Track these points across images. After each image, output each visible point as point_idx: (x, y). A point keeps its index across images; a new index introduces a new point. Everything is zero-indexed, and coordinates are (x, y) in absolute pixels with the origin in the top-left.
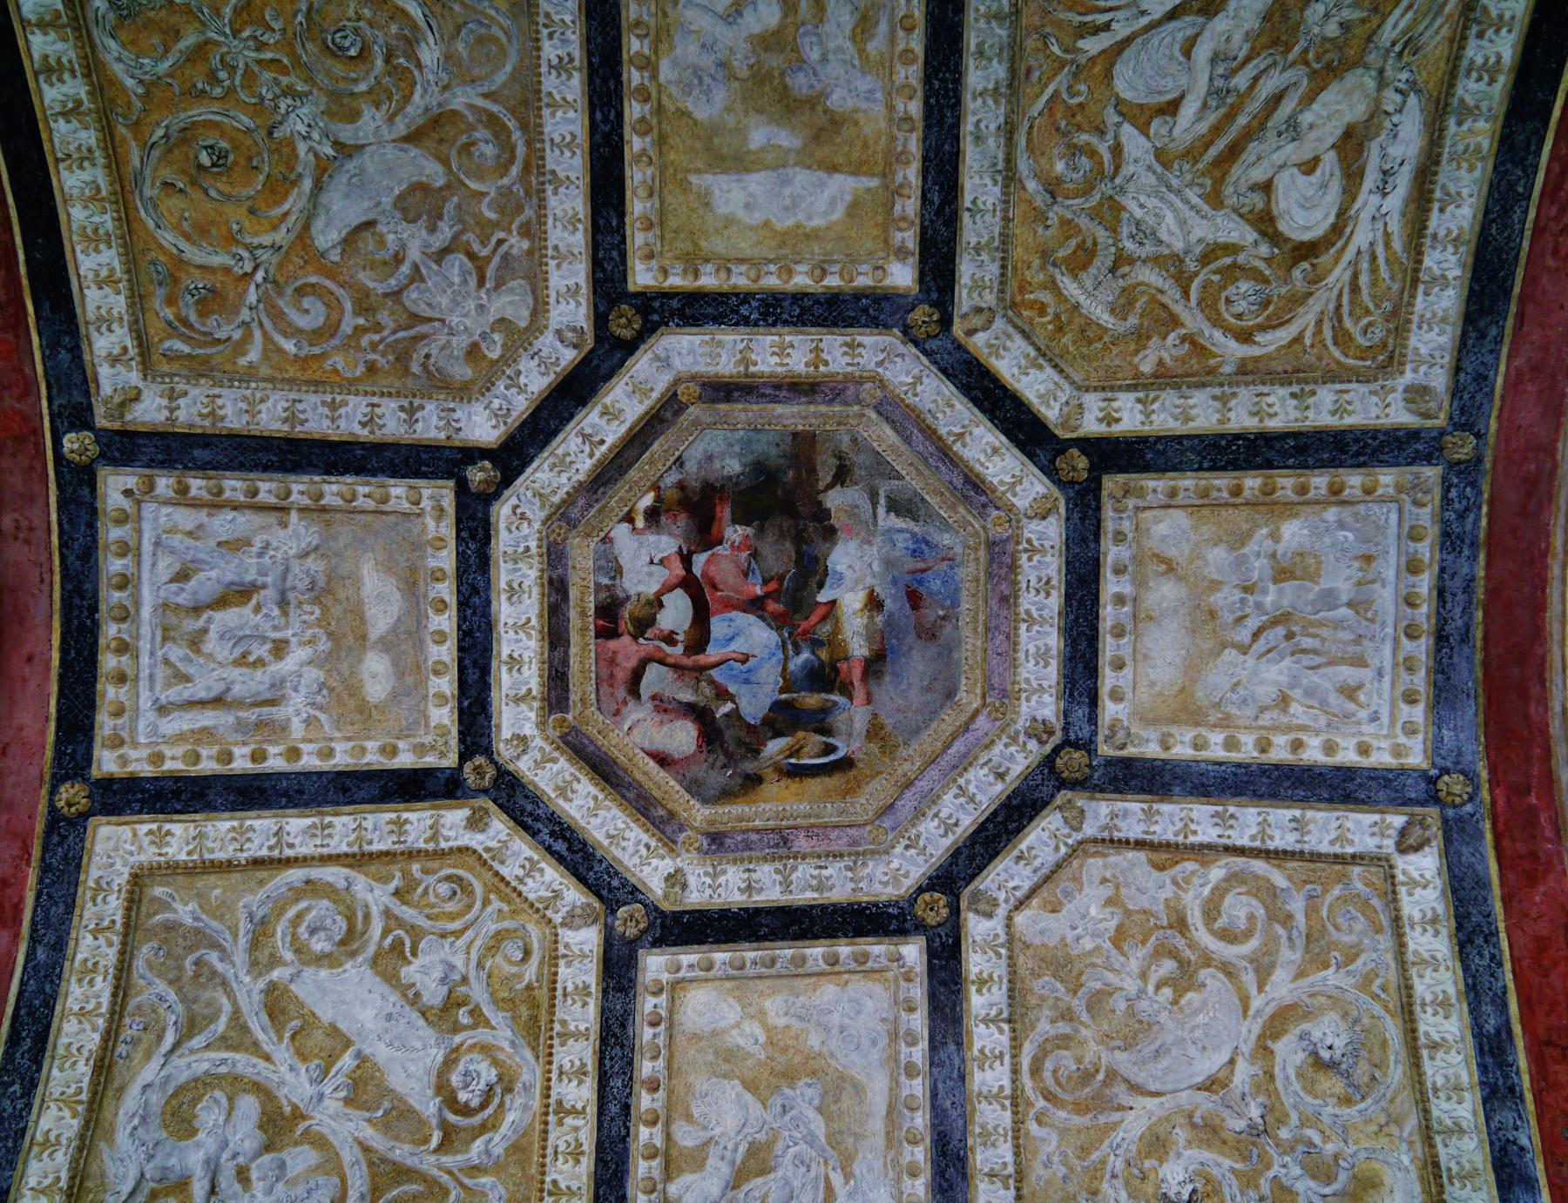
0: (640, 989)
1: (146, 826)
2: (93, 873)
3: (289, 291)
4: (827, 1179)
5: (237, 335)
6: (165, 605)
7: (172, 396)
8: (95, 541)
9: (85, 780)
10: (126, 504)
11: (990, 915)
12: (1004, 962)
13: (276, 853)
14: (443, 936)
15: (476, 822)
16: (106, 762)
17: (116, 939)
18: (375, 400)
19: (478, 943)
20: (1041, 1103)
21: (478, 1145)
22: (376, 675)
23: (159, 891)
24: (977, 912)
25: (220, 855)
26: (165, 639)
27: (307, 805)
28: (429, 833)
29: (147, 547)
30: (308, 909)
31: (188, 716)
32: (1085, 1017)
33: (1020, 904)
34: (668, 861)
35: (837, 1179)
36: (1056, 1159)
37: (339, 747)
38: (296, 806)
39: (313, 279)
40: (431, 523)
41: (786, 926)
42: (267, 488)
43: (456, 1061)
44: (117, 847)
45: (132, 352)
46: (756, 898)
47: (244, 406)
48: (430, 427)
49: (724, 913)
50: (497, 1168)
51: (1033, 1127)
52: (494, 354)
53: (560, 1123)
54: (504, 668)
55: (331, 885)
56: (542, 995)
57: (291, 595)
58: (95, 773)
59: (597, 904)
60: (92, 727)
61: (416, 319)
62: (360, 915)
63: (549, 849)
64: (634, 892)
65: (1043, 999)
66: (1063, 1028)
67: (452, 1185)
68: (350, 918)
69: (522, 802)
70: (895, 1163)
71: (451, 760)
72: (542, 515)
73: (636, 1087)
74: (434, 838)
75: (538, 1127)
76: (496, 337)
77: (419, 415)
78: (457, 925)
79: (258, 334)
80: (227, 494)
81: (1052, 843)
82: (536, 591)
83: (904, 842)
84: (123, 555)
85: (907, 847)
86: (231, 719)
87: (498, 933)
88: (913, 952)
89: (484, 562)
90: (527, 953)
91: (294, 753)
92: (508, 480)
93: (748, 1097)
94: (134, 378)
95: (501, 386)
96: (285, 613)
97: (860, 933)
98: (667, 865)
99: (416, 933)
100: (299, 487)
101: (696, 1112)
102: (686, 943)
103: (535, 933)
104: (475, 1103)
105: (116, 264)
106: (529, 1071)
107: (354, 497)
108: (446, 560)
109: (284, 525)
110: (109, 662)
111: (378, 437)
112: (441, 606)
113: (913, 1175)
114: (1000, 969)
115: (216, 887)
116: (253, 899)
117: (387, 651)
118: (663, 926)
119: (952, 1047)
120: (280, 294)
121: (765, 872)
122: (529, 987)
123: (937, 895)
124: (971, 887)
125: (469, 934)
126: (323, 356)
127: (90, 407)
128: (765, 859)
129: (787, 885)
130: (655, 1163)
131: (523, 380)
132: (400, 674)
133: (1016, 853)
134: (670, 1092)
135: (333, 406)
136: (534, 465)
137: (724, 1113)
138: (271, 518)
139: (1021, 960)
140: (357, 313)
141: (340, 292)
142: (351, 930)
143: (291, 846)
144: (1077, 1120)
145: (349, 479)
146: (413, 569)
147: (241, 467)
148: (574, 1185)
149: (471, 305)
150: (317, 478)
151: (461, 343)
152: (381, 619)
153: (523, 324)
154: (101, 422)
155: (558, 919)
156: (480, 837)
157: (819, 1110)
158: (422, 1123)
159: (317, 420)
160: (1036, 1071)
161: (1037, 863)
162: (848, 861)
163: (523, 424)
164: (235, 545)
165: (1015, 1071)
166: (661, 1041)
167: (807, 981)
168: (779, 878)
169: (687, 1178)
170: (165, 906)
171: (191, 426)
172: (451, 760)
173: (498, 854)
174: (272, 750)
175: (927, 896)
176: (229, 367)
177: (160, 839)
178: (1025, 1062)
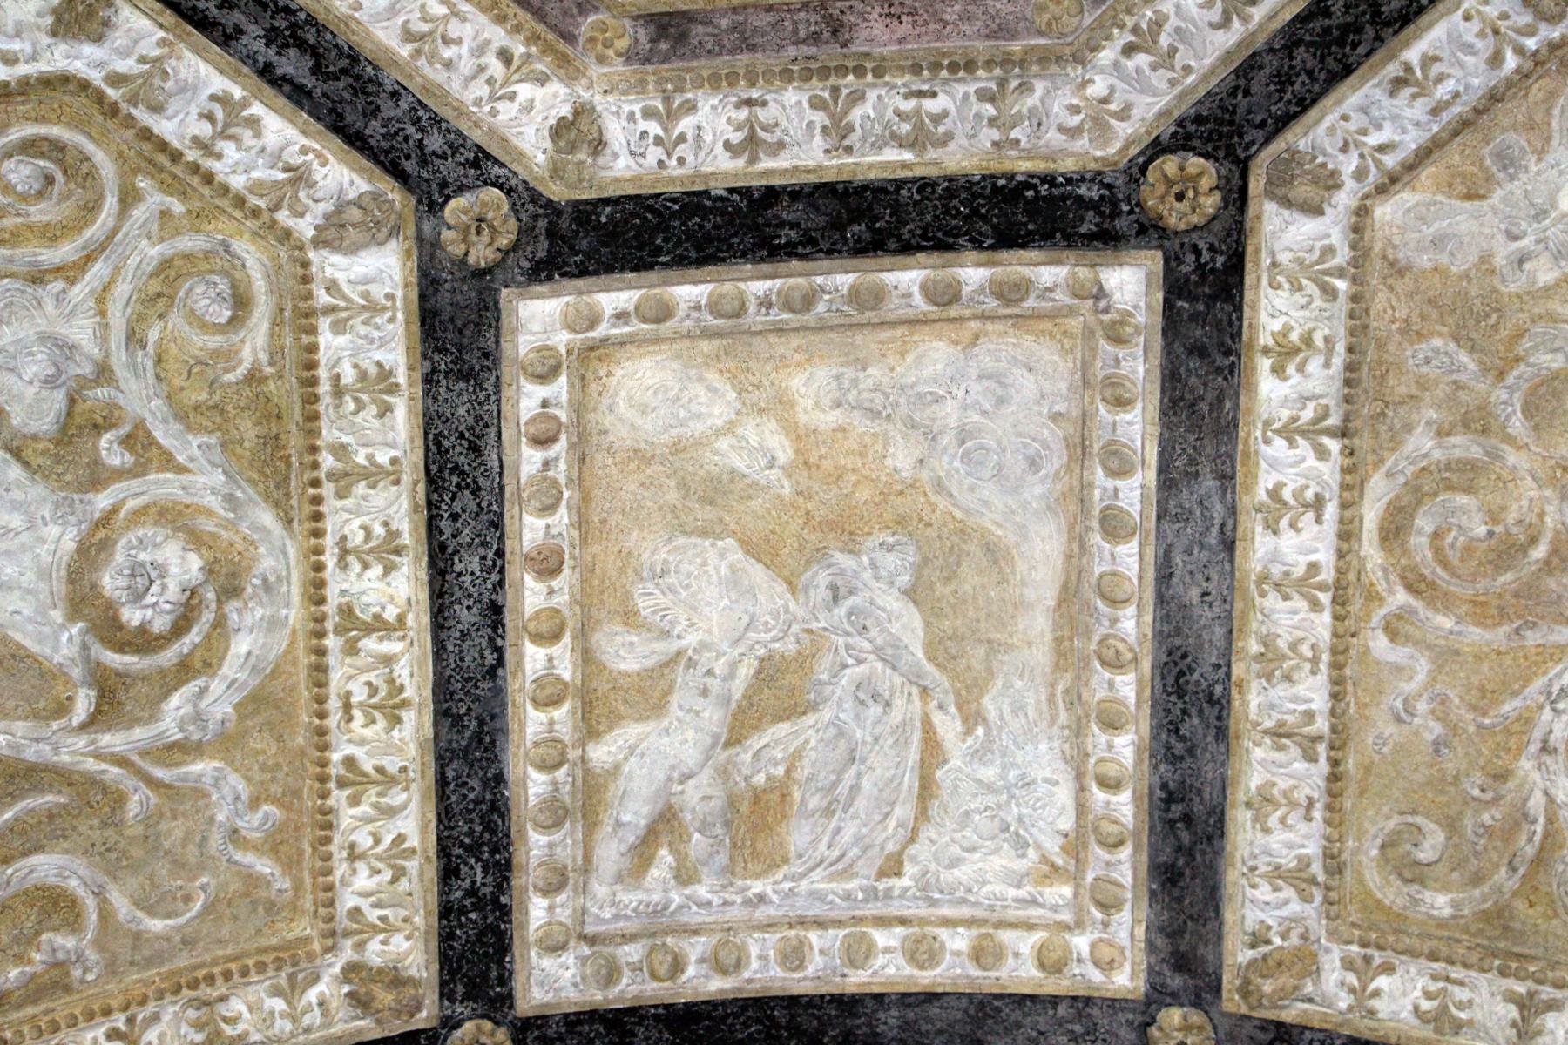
0: (507, 371)
4: (927, 726)
11: (1314, 210)
12: (1342, 305)
14: (37, 278)
19: (122, 289)
20: (1401, 597)
21: (177, 704)
24: (1286, 203)
32: (1517, 425)
33: (1390, 183)
34: (556, 88)
35: (948, 726)
36: (1422, 706)
41: (838, 225)
43: (106, 546)
46: (767, 163)
49: (694, 203)
50: (227, 743)
51: (1380, 645)
53: (351, 649)
56: (284, 391)
59: (394, 193)
63: (266, 72)
64: (481, 163)
65: (1423, 384)
66: (1464, 446)
67: (129, 782)
70: (1074, 699)
73: (511, 573)
75: (305, 660)
78: (66, 251)
81: (1485, 46)
83: (1123, 38)
85: (1129, 50)
87: (165, 264)
88: (1130, 282)
90: (241, 302)
93: (757, 573)
97: (1009, 239)
98: (550, 99)
101: (644, 605)
102: (609, 269)
103: (252, 257)
104: (160, 625)
106: (274, 550)
113: (1111, 724)
114: (1331, 325)
118: (552, 233)
119: (1210, 483)
121: (790, 107)
122: (254, 377)
123: (1195, 163)
124: (1278, 146)
125: (99, 270)
128: (787, 76)
129: (838, 133)
130: (561, 713)
133: (1393, 69)
134: (587, 572)
137: (709, 604)
139: (1380, 301)
144: (1475, 633)
148: (392, 764)
155: (305, 228)
156: (88, 49)
157: (911, 594)
158: (48, 675)
160: (1394, 530)
161: (1442, 91)
162: (985, 79)
165: (1347, 534)
166: (560, 472)
167: (886, 334)
168: (819, 118)
169: (630, 732)
173: (148, 86)
175: (1169, 165)
178: (1371, 515)
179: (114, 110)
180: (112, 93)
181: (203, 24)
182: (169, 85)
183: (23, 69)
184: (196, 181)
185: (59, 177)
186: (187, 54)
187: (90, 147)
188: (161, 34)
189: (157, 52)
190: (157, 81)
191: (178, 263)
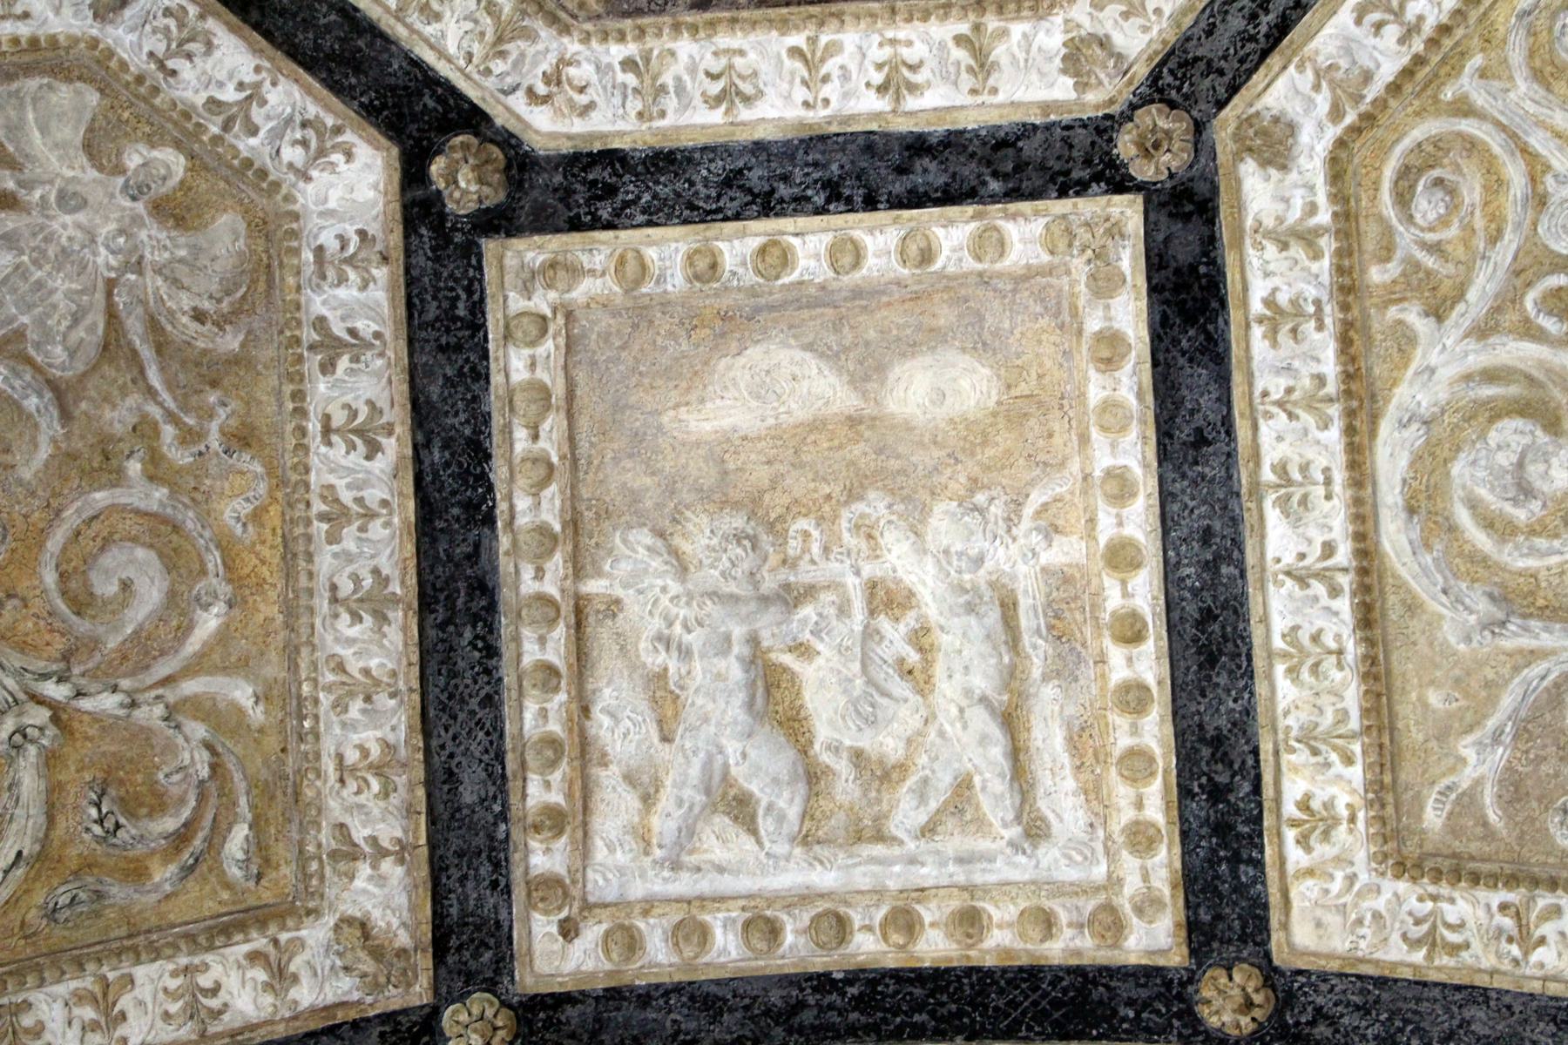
1: (1288, 851)
2: (1398, 955)
3: (83, 626)
5: (198, 730)
6: (805, 840)
7: (348, 853)
8: (678, 988)
9: (1192, 978)
10: (592, 933)
13: (1345, 581)
14: (1540, 201)
15: (1273, 144)
16: (1153, 938)
17: (1544, 900)
18: (314, 426)
22: (937, 389)
23: (1433, 818)
25: (1352, 698)
26: (880, 837)
27: (1235, 522)
28: (1297, 251)
29: (684, 885)
30: (1473, 504)
31: (1045, 780)
37: (1103, 460)
38: (1238, 544)
39: (50, 578)
40: (583, 290)
42: (533, 646)
44: (1336, 906)
45: (259, 942)
47: (356, 708)
48: (365, 302)
52: (173, 162)
54: (911, 103)
55: (1417, 460)
57: (769, 584)
58: (1177, 958)
60: (1078, 971)
61: (113, 345)
62: (1488, 391)
68: (1496, 412)
69: (1222, 40)
71: (1128, 211)
72: (545, 32)
74: (1308, 238)
76: (133, 160)
77: (338, 330)
78: (1515, 174)
79: (190, 687)
80: (555, 727)
82: (724, 40)
84: (704, 933)
86: (1049, 692)
87: (1537, 75)
89: (666, 161)
91: (1121, 557)
92: (472, 118)
94: (316, 934)
95: (249, 145)
96: (810, 592)
99: (1534, 262)
100: (527, 579)
105: (62, 989)
107: (542, 460)
108: (667, 250)
109: (614, 606)
110: (935, 947)
111: (398, 416)
112: (774, 257)
115: (1425, 700)
116: (1450, 621)
117: (881, 369)
120: (94, 644)
125: (1538, 141)
126: (226, 545)
127: (388, 1017)
131: (230, 95)
132: (934, 338)
135: (337, 517)
136: (429, 57)
138: (602, 635)
140: (118, 478)
141: (72, 517)
142: (1523, 409)
143: (1329, 549)
145: (499, 472)
146: (692, 321)
147: (492, 701)
149: (65, 225)
150: (504, 542)
151: (154, 238)
152: (818, 388)
153: (93, 98)
154: (420, 993)
156: (1305, 136)
159: (376, 546)
163: (336, 88)
164: (665, 703)
170: (1468, 802)
171: (410, 811)
172: (1128, 211)
173: (1344, 85)
174: (1114, 600)
176: (272, 742)
177: (1317, 822)
179: (1368, 119)
180: (1350, 118)
181: (1283, 28)
182: (1344, 63)
183: (1321, 198)
184: (1447, 43)
185: (1436, 173)
186: (1313, 45)
187: (1407, 142)
188: (1292, 69)
189: (1310, 74)
190: (1340, 75)
191: (1538, 63)
